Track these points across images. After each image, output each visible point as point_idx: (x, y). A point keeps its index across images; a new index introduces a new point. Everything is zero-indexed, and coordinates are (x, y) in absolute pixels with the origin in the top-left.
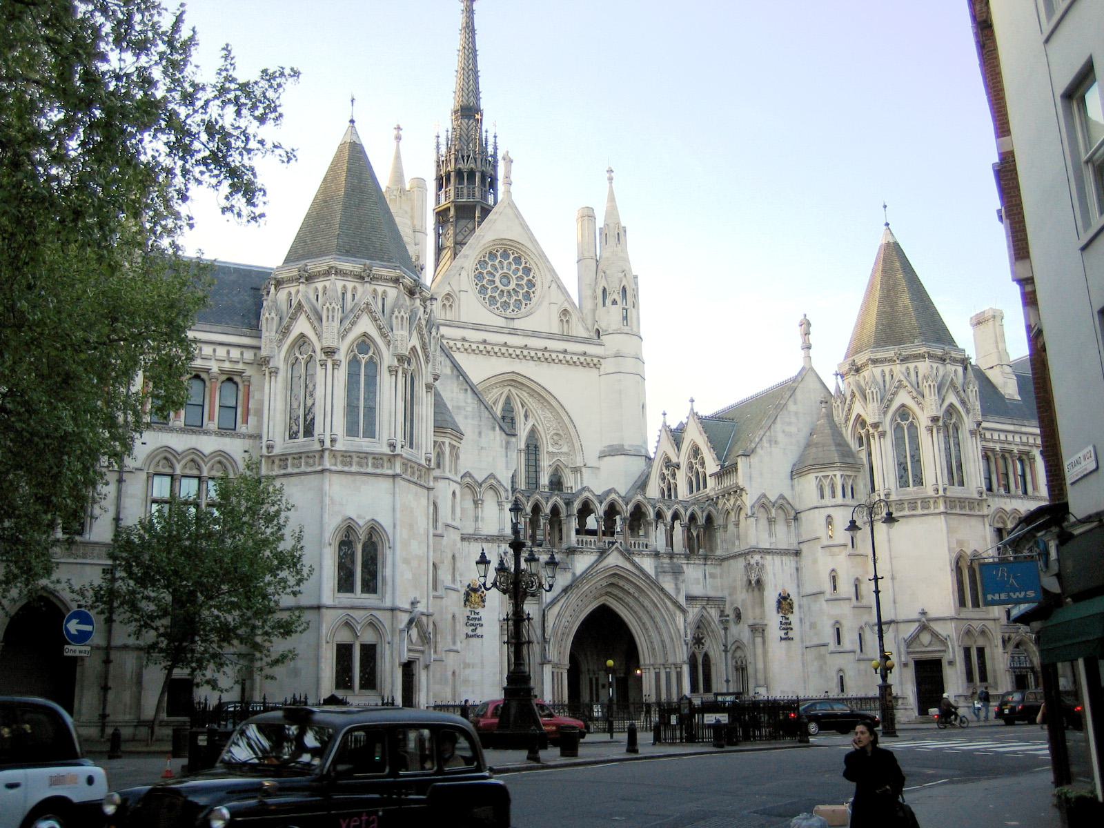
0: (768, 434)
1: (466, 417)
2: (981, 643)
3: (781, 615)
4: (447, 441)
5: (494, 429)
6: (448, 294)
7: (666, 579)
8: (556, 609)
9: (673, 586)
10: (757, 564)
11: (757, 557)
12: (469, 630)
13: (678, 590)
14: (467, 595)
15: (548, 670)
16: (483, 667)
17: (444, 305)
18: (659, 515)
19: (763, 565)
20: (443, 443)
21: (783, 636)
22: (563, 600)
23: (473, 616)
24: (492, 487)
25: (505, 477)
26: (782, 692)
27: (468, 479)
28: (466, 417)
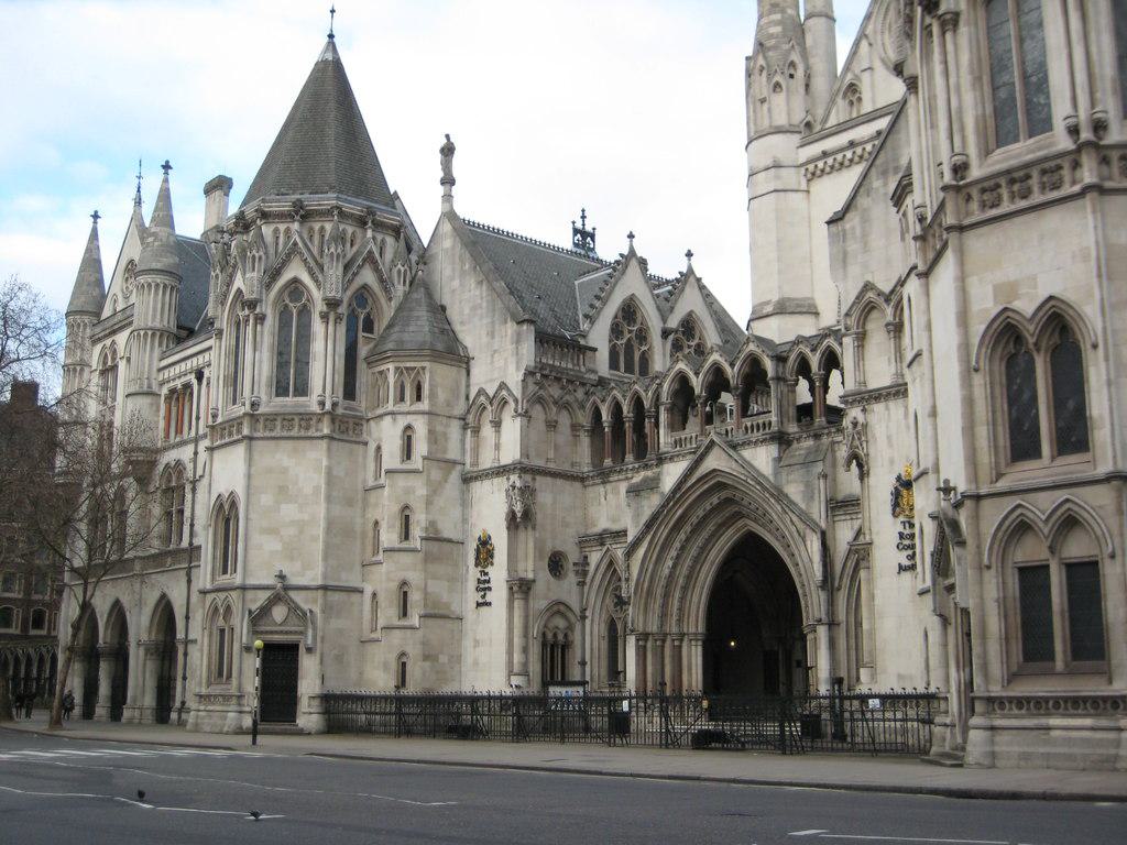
0: (878, 162)
1: (481, 319)
2: (1077, 548)
3: (902, 518)
4: (391, 366)
5: (506, 322)
6: (852, 85)
7: (792, 477)
8: (641, 552)
9: (802, 488)
10: (855, 424)
11: (855, 413)
12: (478, 597)
13: (809, 497)
14: (478, 551)
15: (631, 642)
16: (491, 645)
17: (851, 103)
18: (804, 368)
19: (865, 426)
20: (388, 369)
21: (906, 563)
22: (649, 537)
23: (483, 578)
24: (505, 402)
25: (514, 379)
26: (900, 677)
27: (482, 398)
28: (481, 319)
